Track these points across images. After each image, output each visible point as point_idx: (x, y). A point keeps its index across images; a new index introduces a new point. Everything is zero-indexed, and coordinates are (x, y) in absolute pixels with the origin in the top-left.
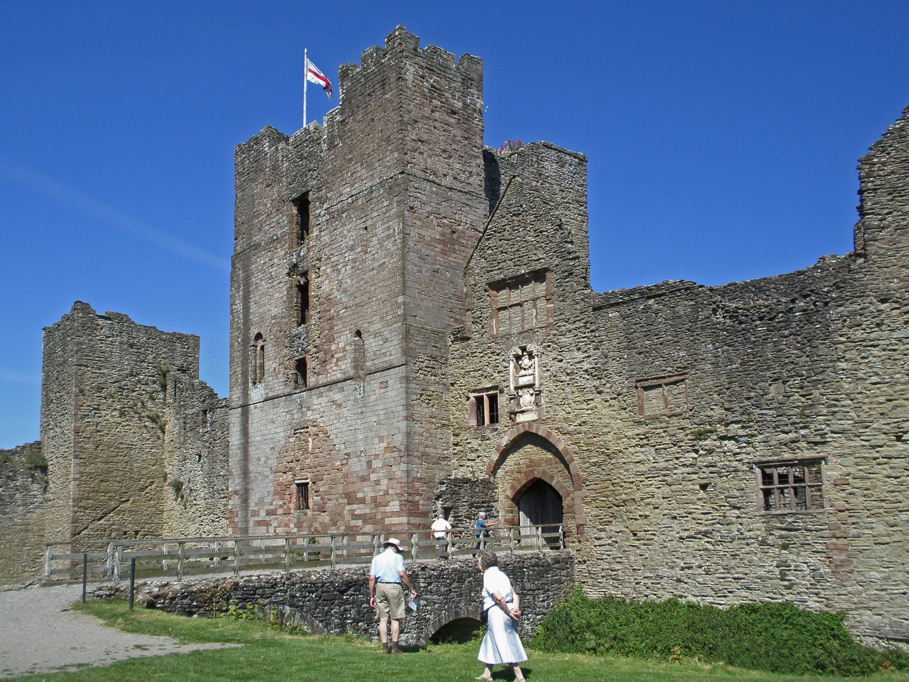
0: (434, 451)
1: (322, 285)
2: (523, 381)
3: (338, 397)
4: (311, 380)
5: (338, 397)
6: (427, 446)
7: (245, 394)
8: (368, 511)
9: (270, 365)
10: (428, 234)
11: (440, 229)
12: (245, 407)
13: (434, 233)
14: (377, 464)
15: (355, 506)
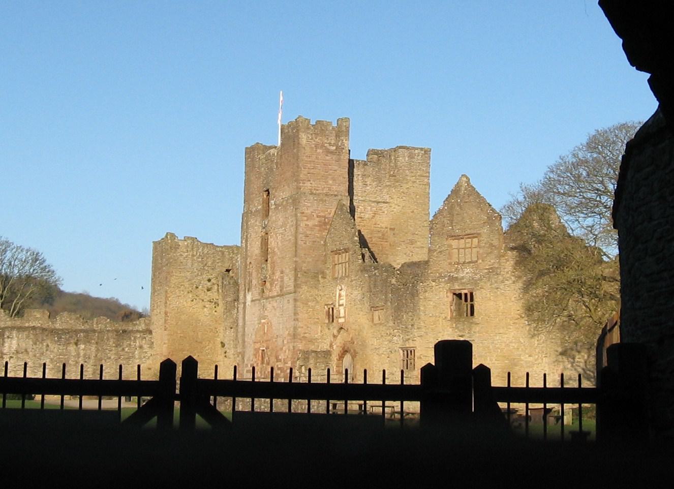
0: (309, 335)
1: (272, 243)
2: (341, 302)
3: (275, 305)
4: (267, 293)
5: (275, 305)
6: (305, 333)
7: (245, 296)
8: (282, 366)
9: (254, 282)
10: (310, 223)
11: (318, 219)
12: (245, 303)
13: (316, 221)
14: (285, 342)
15: (278, 363)
